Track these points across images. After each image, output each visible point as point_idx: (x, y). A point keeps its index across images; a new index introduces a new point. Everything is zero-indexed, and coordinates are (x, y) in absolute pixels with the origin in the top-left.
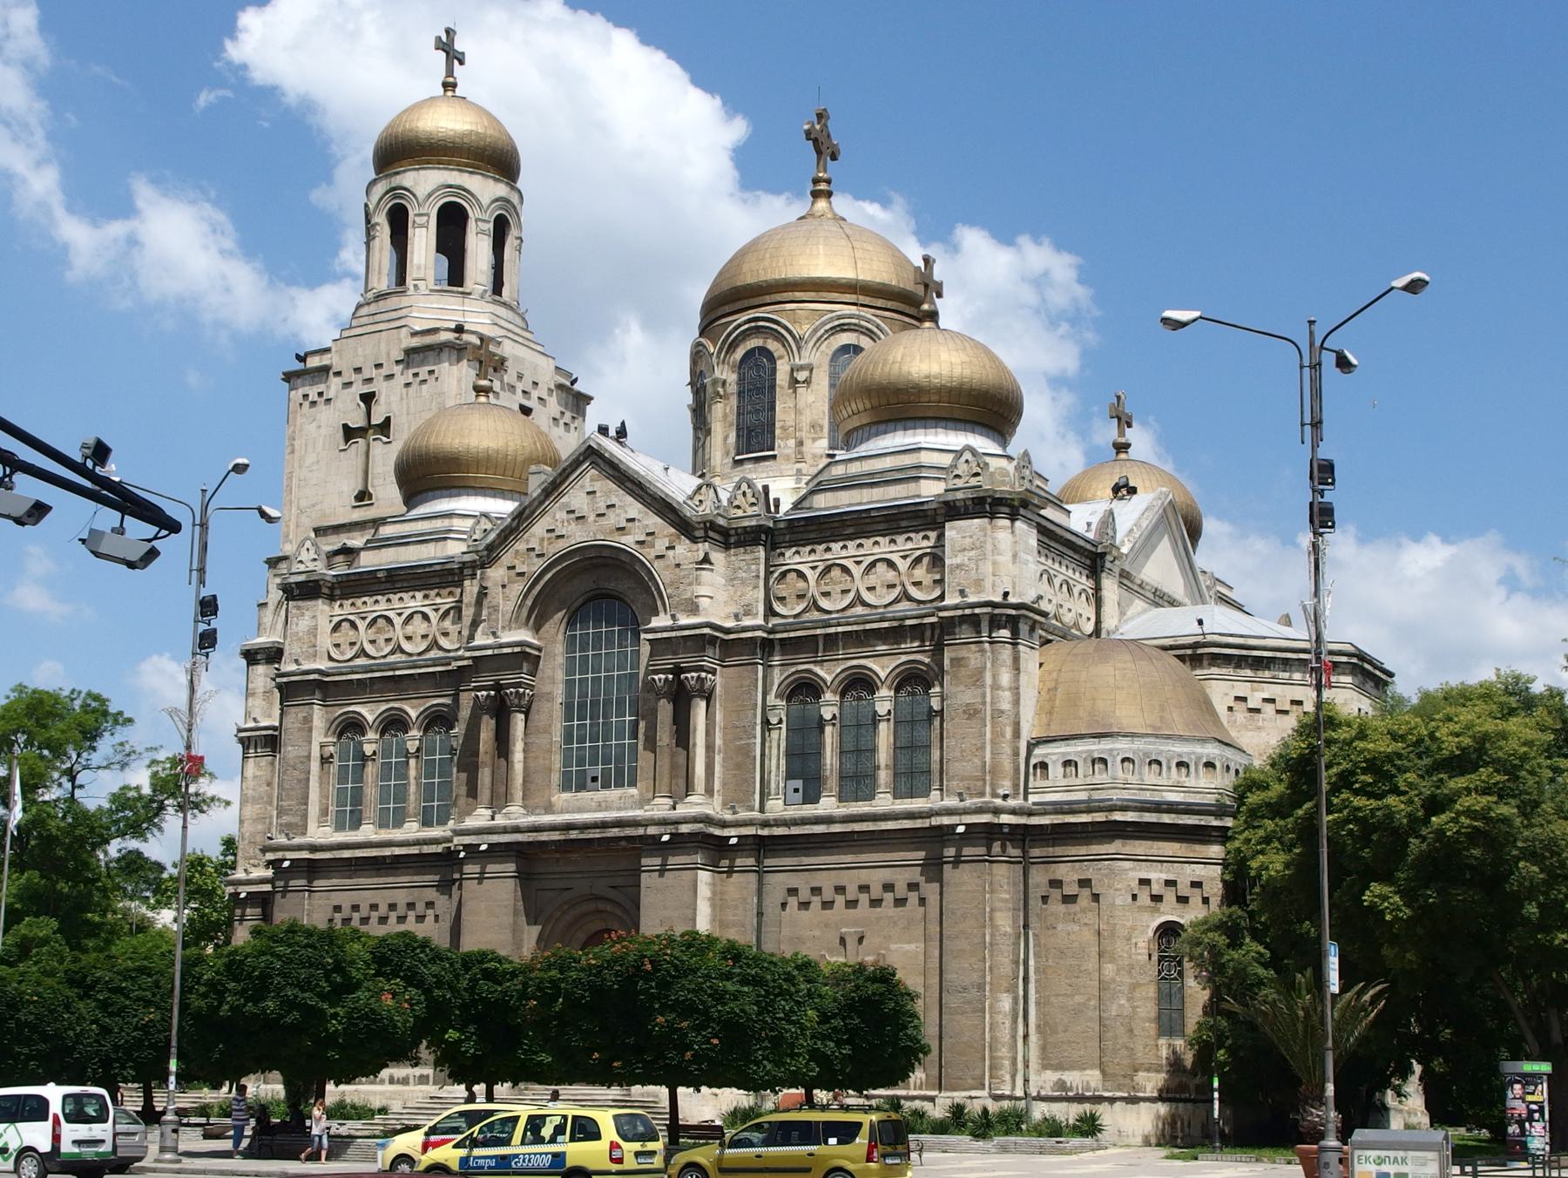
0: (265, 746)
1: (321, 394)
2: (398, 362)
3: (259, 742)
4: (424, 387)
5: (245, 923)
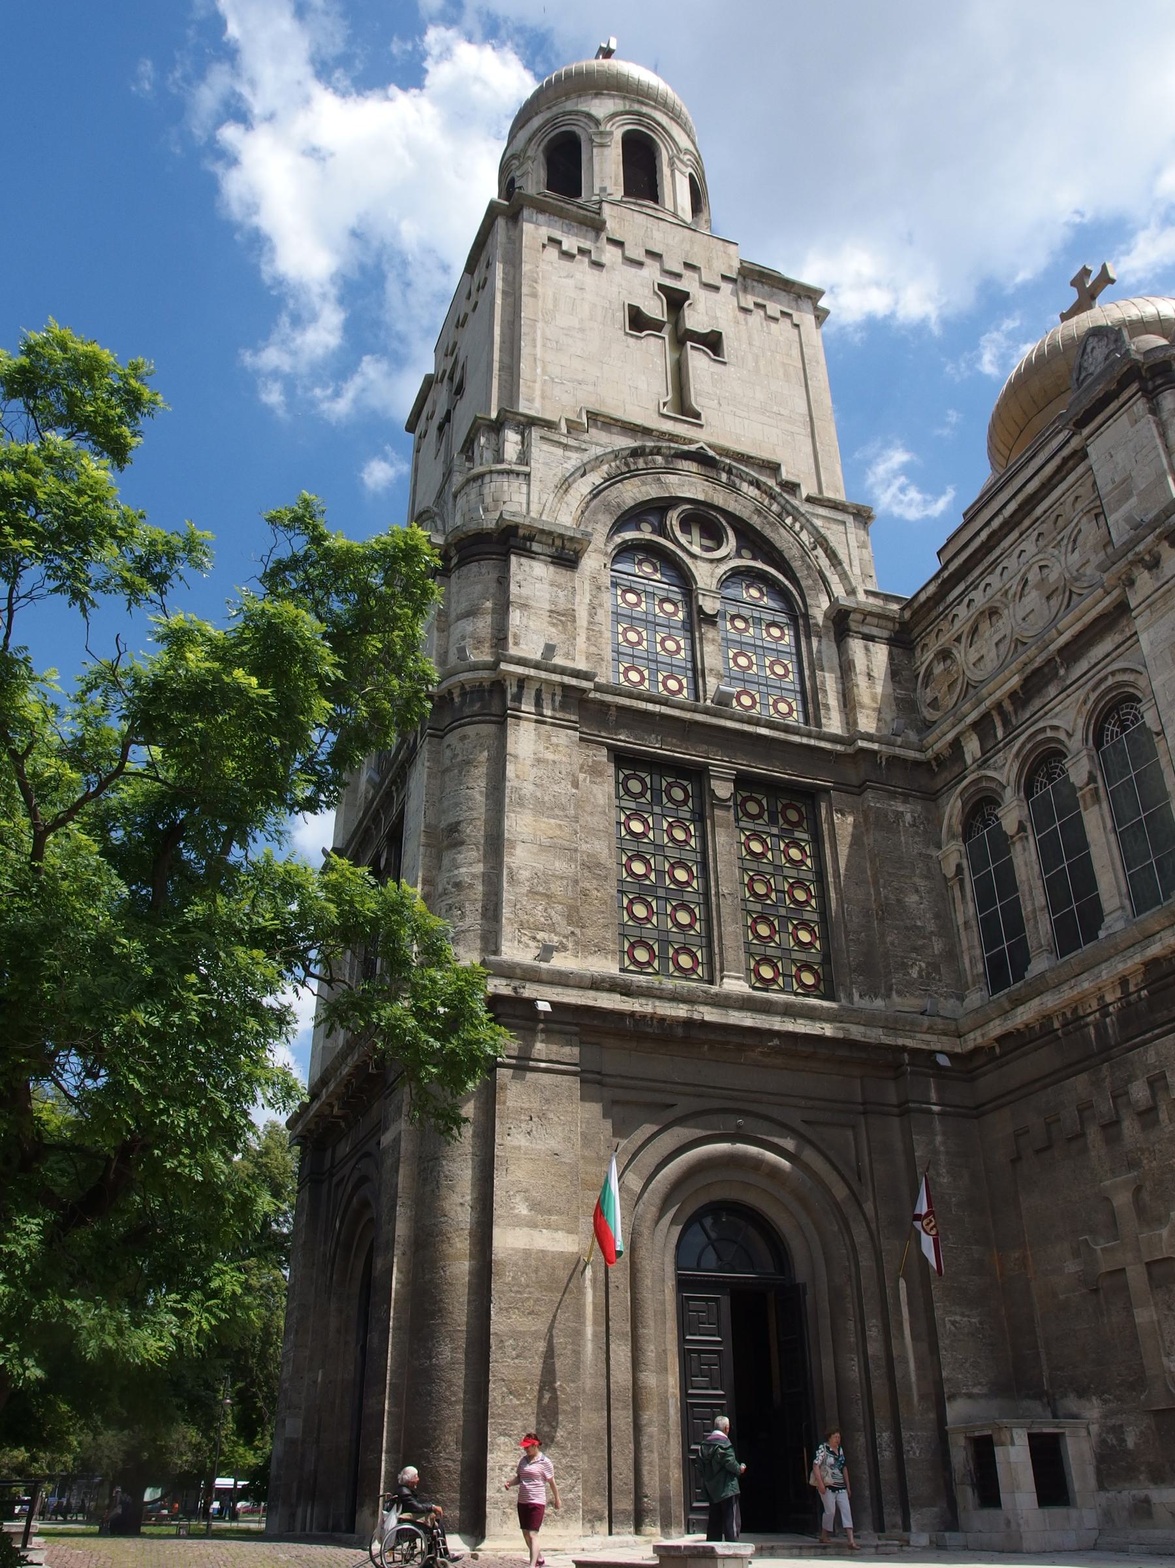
0: (564, 707)
1: (582, 251)
2: (724, 277)
3: (546, 697)
4: (773, 325)
5: (530, 1076)
